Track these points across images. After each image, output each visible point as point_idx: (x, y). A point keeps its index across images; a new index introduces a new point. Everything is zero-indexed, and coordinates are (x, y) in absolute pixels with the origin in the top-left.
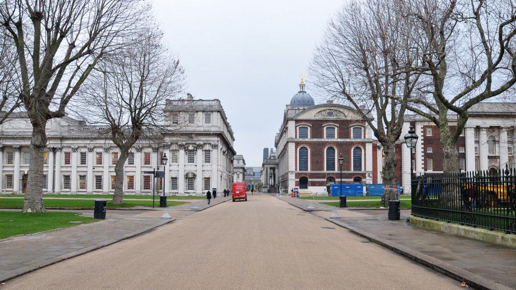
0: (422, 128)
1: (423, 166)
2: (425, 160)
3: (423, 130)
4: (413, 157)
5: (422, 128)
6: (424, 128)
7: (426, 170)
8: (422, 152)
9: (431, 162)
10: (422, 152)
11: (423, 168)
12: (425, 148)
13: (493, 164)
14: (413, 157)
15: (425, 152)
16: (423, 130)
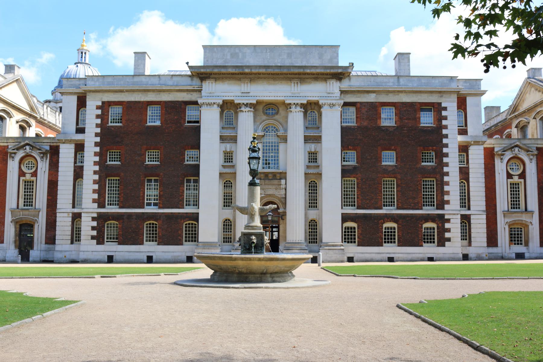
0: (98, 108)
1: (96, 196)
2: (101, 182)
3: (99, 112)
4: (78, 173)
5: (98, 108)
6: (105, 106)
7: (101, 205)
8: (95, 163)
9: (112, 183)
10: (95, 163)
11: (94, 201)
12: (101, 155)
13: (270, 192)
14: (78, 173)
15: (101, 163)
16: (99, 112)
